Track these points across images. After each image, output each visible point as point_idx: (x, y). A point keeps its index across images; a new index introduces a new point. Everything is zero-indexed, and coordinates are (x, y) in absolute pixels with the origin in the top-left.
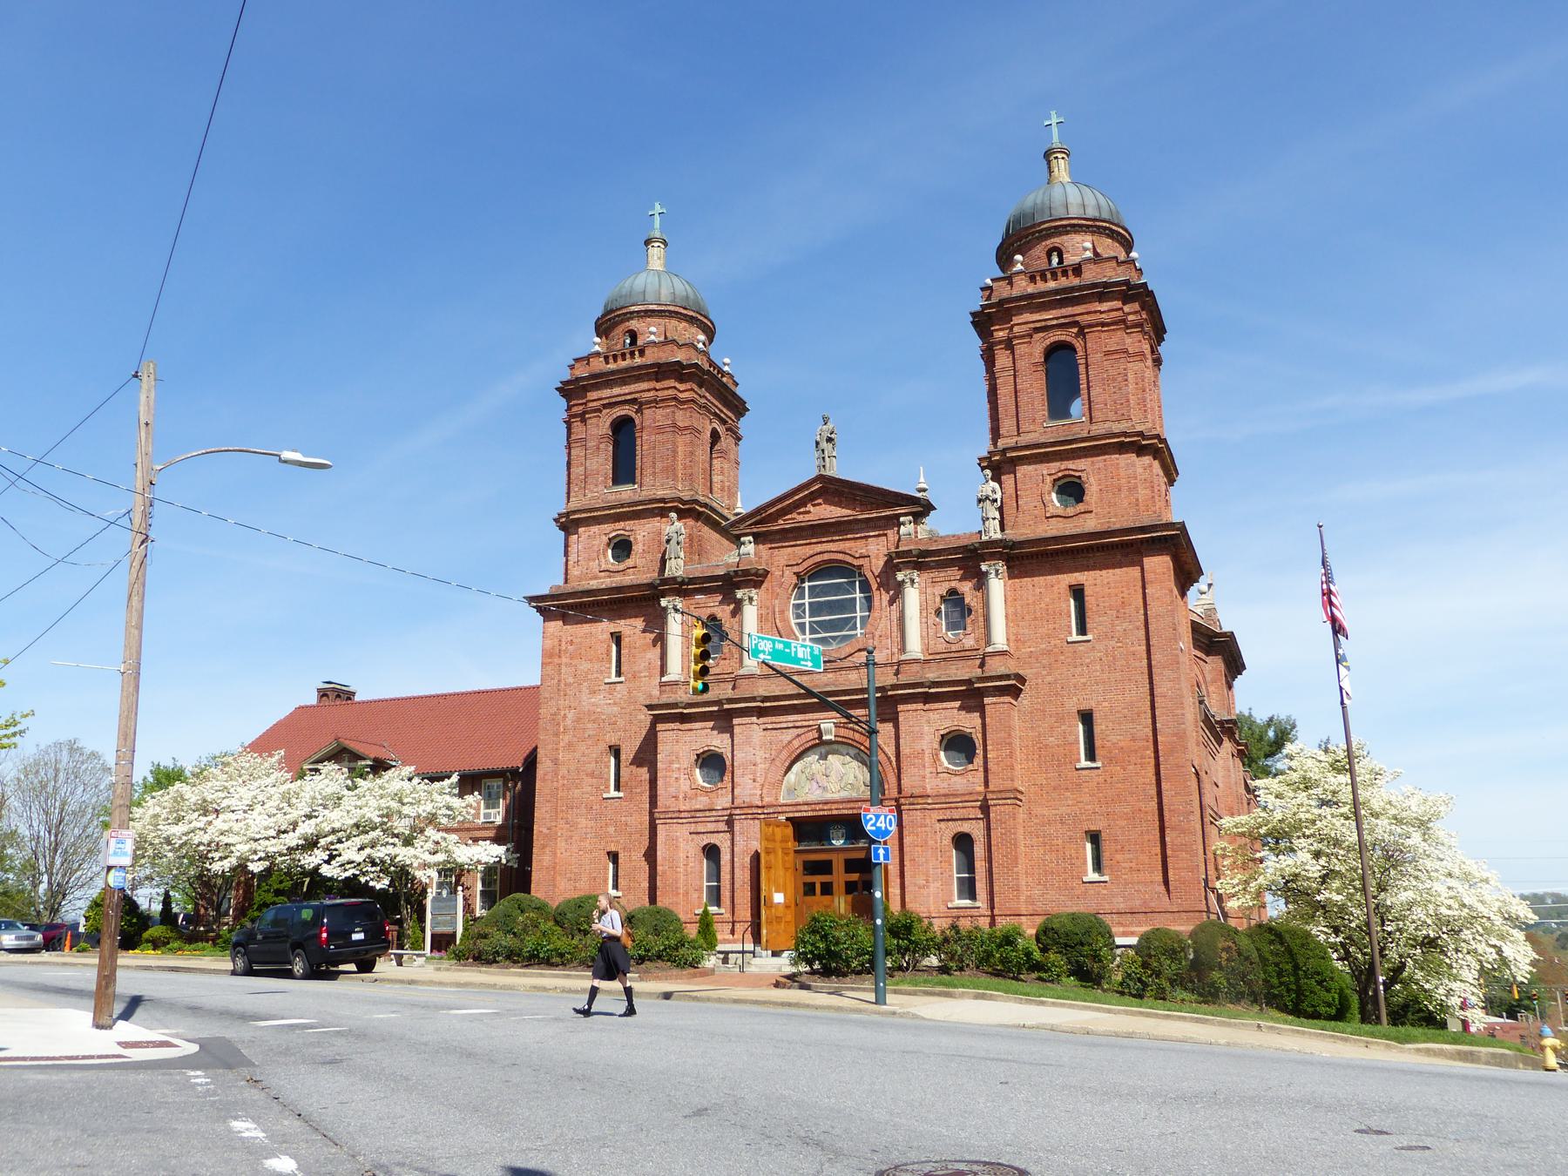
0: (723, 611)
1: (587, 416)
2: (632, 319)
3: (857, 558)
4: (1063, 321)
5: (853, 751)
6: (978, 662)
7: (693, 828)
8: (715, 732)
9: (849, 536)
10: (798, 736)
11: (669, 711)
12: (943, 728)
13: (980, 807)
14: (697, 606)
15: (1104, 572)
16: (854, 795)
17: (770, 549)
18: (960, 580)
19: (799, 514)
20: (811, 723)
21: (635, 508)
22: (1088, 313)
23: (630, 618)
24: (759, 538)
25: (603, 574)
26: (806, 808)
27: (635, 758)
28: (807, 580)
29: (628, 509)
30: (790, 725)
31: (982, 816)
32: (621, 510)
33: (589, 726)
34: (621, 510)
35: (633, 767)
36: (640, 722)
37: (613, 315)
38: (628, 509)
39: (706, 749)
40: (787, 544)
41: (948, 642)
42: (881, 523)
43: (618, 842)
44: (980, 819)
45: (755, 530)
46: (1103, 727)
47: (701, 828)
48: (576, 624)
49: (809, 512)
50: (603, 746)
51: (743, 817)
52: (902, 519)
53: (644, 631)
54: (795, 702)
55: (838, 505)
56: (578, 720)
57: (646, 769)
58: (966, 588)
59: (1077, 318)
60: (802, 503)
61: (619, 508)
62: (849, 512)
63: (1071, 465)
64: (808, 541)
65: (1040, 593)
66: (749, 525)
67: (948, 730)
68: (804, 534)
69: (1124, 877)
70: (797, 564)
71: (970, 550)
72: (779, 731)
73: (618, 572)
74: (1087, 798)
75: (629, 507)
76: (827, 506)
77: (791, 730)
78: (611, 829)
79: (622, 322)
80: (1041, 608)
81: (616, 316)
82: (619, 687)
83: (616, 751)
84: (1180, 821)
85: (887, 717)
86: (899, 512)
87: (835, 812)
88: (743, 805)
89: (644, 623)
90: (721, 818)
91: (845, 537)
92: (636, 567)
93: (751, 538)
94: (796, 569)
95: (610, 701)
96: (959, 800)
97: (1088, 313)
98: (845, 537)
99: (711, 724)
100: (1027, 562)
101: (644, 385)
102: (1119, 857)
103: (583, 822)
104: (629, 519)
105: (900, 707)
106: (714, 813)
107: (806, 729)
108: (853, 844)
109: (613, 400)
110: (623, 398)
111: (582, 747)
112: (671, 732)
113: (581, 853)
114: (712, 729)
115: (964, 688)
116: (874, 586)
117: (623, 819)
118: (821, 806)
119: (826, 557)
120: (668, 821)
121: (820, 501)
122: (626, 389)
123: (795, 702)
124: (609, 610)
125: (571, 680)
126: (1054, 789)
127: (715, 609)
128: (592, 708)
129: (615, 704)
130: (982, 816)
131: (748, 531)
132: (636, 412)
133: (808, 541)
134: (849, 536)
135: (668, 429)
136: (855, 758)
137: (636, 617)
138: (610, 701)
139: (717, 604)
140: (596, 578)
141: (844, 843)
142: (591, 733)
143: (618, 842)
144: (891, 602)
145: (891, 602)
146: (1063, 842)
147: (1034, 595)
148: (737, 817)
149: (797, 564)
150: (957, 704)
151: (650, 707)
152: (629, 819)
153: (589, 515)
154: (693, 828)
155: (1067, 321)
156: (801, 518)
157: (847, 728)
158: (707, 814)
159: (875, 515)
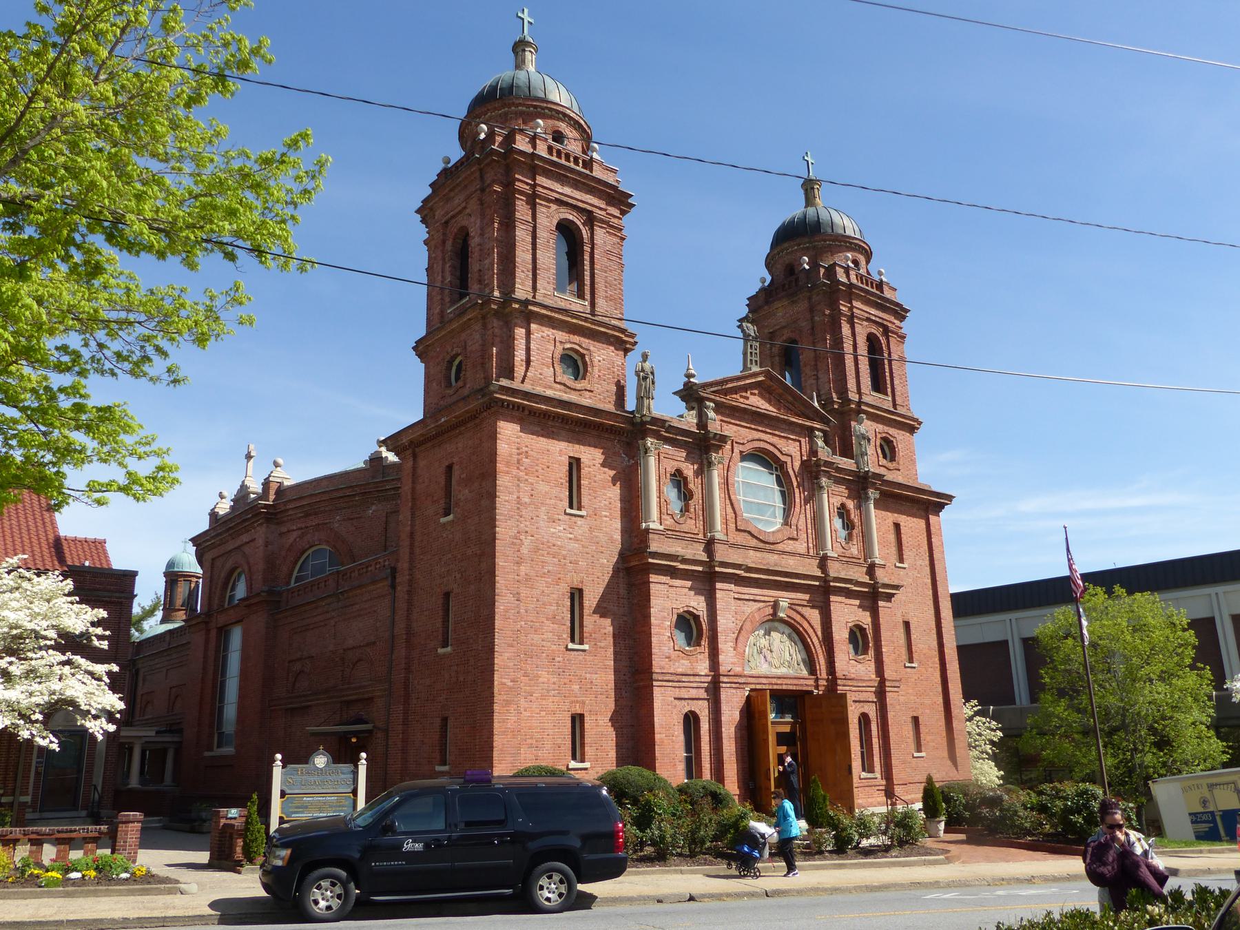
0: (687, 468)
1: (537, 200)
2: (563, 121)
3: (783, 454)
4: (877, 319)
5: (788, 630)
6: (865, 569)
7: (678, 693)
8: (693, 593)
9: (777, 433)
11: (669, 563)
13: (875, 693)
14: (667, 456)
15: (909, 518)
16: (791, 672)
17: (721, 421)
18: (847, 498)
19: (741, 397)
20: (766, 599)
22: (890, 322)
23: (590, 446)
24: (719, 408)
25: (558, 386)
26: (764, 681)
27: (598, 606)
29: (589, 325)
31: (875, 700)
32: (583, 323)
33: (549, 559)
34: (583, 323)
35: (596, 617)
36: (602, 565)
37: (545, 105)
38: (589, 325)
40: (733, 421)
41: (843, 548)
42: (797, 430)
43: (583, 703)
44: (873, 702)
45: (718, 399)
47: (684, 693)
48: (533, 434)
49: (747, 398)
50: (564, 589)
51: (728, 685)
53: (603, 465)
54: (762, 576)
55: (770, 402)
56: (536, 550)
57: (608, 621)
58: (850, 504)
59: (885, 323)
60: (745, 388)
61: (582, 320)
62: (771, 408)
63: (892, 431)
64: (748, 425)
66: (713, 392)
68: (746, 417)
70: (743, 444)
71: (859, 477)
72: (742, 602)
73: (575, 390)
74: (911, 691)
75: (592, 324)
76: (760, 399)
77: (751, 603)
78: (576, 687)
79: (559, 119)
81: (547, 108)
82: (579, 521)
83: (576, 595)
85: (816, 604)
87: (784, 687)
88: (730, 673)
89: (603, 457)
90: (703, 685)
91: (774, 432)
92: (592, 391)
93: (712, 405)
94: (741, 448)
95: (571, 536)
97: (890, 322)
98: (774, 432)
99: (689, 584)
101: (595, 201)
102: (928, 738)
103: (544, 676)
104: (584, 336)
105: (833, 598)
106: (697, 679)
108: (781, 718)
109: (565, 199)
110: (574, 202)
111: (541, 585)
112: (663, 586)
113: (543, 713)
114: (690, 589)
115: (867, 590)
116: (795, 484)
117: (588, 676)
119: (762, 445)
120: (664, 683)
121: (756, 392)
122: (578, 194)
123: (762, 576)
124: (570, 430)
125: (527, 500)
127: (681, 464)
128: (553, 540)
129: (576, 540)
130: (875, 700)
131: (713, 397)
132: (584, 224)
133: (748, 425)
134: (777, 433)
135: (614, 258)
136: (789, 637)
137: (595, 447)
138: (571, 536)
139: (683, 460)
140: (551, 388)
141: (775, 717)
142: (550, 568)
143: (583, 703)
144: (807, 501)
145: (807, 501)
148: (724, 685)
149: (743, 444)
150: (857, 602)
152: (594, 676)
153: (549, 313)
154: (678, 693)
155: (880, 321)
156: (742, 400)
157: (793, 609)
158: (692, 679)
159: (800, 422)
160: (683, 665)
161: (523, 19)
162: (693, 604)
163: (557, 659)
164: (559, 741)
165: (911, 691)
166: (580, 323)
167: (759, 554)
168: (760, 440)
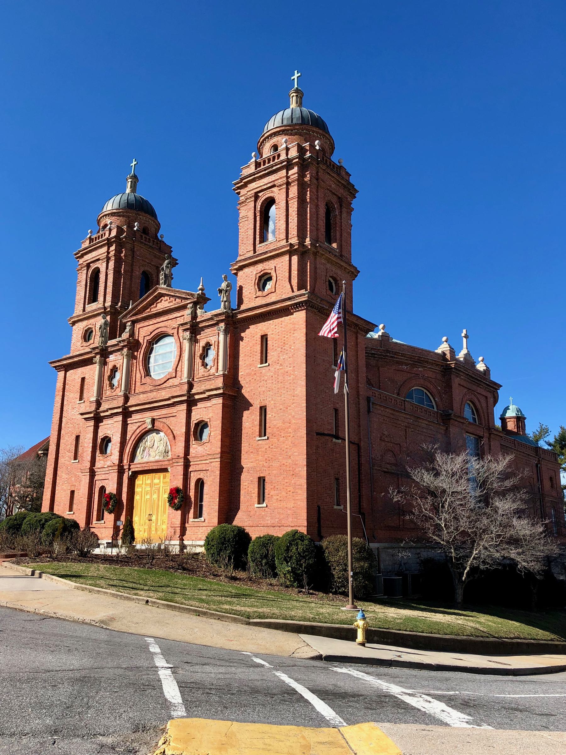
10: (139, 427)
30: (137, 421)
39: (105, 435)
46: (270, 416)
51: (112, 471)
69: (274, 504)
74: (260, 458)
80: (248, 350)
84: (300, 471)
96: (199, 460)
100: (244, 323)
102: (272, 493)
106: (104, 469)
118: (145, 465)
119: (159, 330)
126: (247, 453)
146: (248, 484)
151: (82, 414)
158: (102, 470)
160: (101, 463)
161: (135, 165)
163: (69, 468)
164: (66, 502)
165: (260, 458)
167: (145, 395)
168: (158, 328)
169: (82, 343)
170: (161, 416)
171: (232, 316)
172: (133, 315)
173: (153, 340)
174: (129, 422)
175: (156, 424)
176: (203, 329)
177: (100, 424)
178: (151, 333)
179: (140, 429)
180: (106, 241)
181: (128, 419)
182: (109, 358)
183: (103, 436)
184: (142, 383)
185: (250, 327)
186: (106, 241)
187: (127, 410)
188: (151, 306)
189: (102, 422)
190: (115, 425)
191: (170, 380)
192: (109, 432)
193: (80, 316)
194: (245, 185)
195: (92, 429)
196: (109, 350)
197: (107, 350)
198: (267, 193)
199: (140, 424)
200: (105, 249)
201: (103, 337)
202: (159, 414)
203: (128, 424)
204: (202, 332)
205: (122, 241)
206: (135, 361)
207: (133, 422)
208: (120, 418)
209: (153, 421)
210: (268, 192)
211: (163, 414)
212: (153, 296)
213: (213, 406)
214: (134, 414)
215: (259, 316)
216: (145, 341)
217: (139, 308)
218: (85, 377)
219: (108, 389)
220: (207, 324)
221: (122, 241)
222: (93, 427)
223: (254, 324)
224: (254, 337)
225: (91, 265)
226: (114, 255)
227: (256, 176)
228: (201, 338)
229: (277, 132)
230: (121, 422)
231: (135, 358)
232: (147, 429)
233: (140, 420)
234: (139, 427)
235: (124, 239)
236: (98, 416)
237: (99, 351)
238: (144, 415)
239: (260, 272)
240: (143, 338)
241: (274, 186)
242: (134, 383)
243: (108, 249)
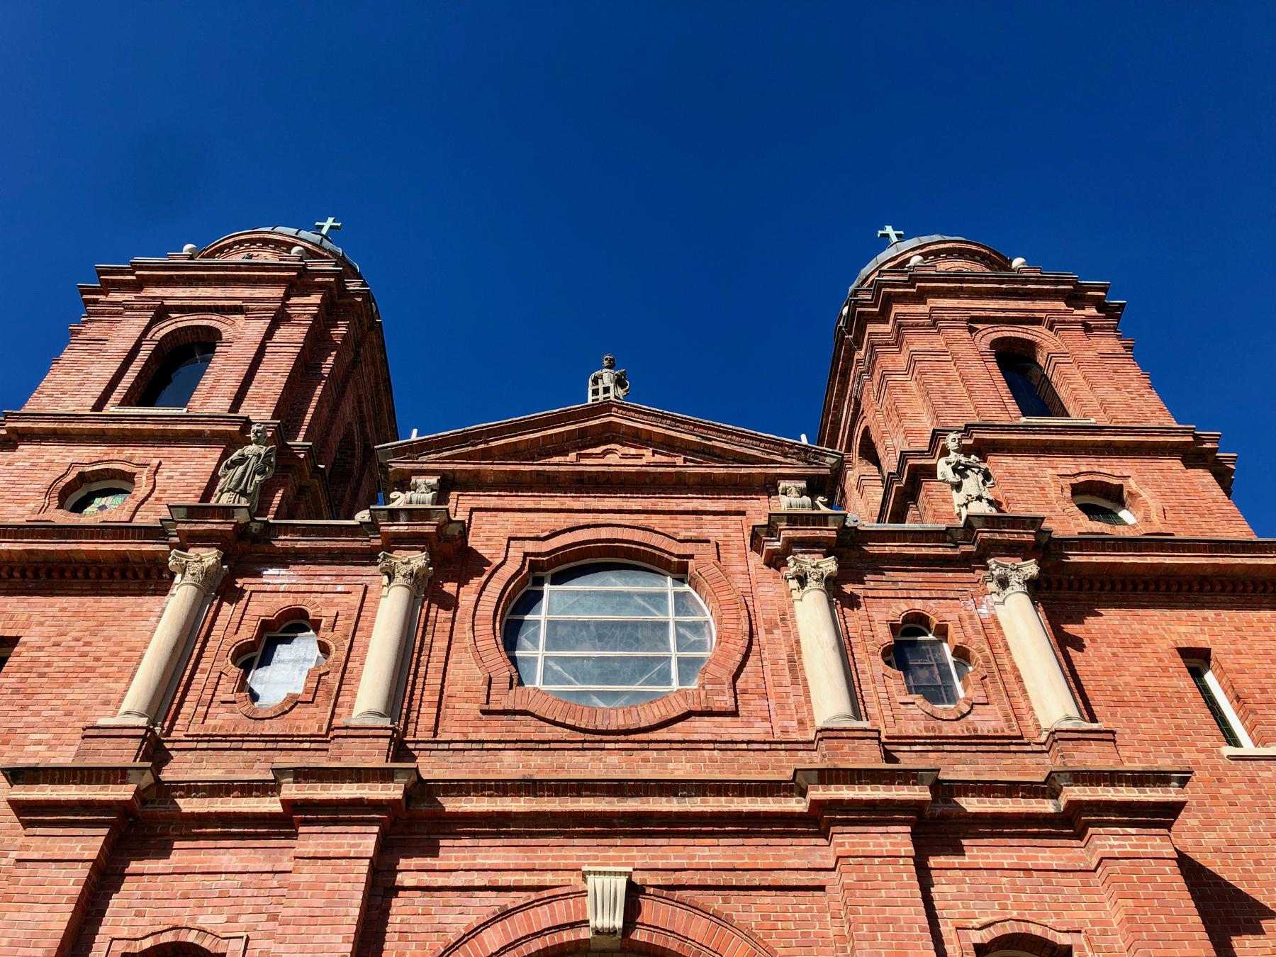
10: (506, 914)
12: (975, 923)
21: (169, 427)
28: (549, 579)
30: (478, 880)
32: (138, 426)
39: (168, 938)
52: (783, 484)
65: (1114, 655)
66: (439, 458)
67: (996, 932)
86: (779, 471)
94: (531, 547)
107: (533, 896)
119: (604, 533)
147: (1101, 658)
162: (203, 920)
166: (129, 426)
169: (43, 509)
170: (685, 878)
171: (1047, 545)
172: (468, 457)
173: (551, 564)
174: (404, 879)
175: (651, 910)
176: (879, 564)
177: (134, 866)
178: (554, 534)
179: (517, 926)
180: (295, 274)
181: (403, 863)
182: (259, 575)
183: (148, 944)
184: (493, 707)
185: (1102, 611)
186: (295, 274)
187: (424, 807)
188: (550, 456)
189: (164, 851)
190: (293, 878)
191: (697, 722)
192: (206, 920)
193: (78, 418)
194: (920, 297)
195: (72, 881)
196: (278, 544)
197: (268, 542)
198: (996, 329)
199: (509, 900)
200: (278, 292)
201: (243, 493)
202: (673, 862)
203: (395, 890)
204: (869, 577)
205: (346, 301)
206: (444, 615)
207: (426, 879)
208: (365, 841)
209: (634, 892)
210: (1016, 329)
211: (696, 862)
212: (582, 425)
213: (1116, 867)
214: (457, 836)
215: (1157, 583)
216: (516, 551)
217: (494, 444)
218: (17, 638)
219: (221, 696)
220: (913, 551)
221: (346, 301)
222: (82, 871)
223: (1119, 607)
224: (1138, 645)
225: (173, 316)
226: (315, 317)
227: (964, 285)
228: (870, 593)
229: (969, 250)
230: (363, 867)
231: (451, 603)
232: (585, 934)
233: (527, 879)
234: (506, 914)
235: (360, 300)
236: (160, 810)
237: (230, 527)
238: (540, 852)
239: (1074, 475)
240: (505, 542)
241: (1038, 322)
242: (433, 698)
243: (287, 296)
